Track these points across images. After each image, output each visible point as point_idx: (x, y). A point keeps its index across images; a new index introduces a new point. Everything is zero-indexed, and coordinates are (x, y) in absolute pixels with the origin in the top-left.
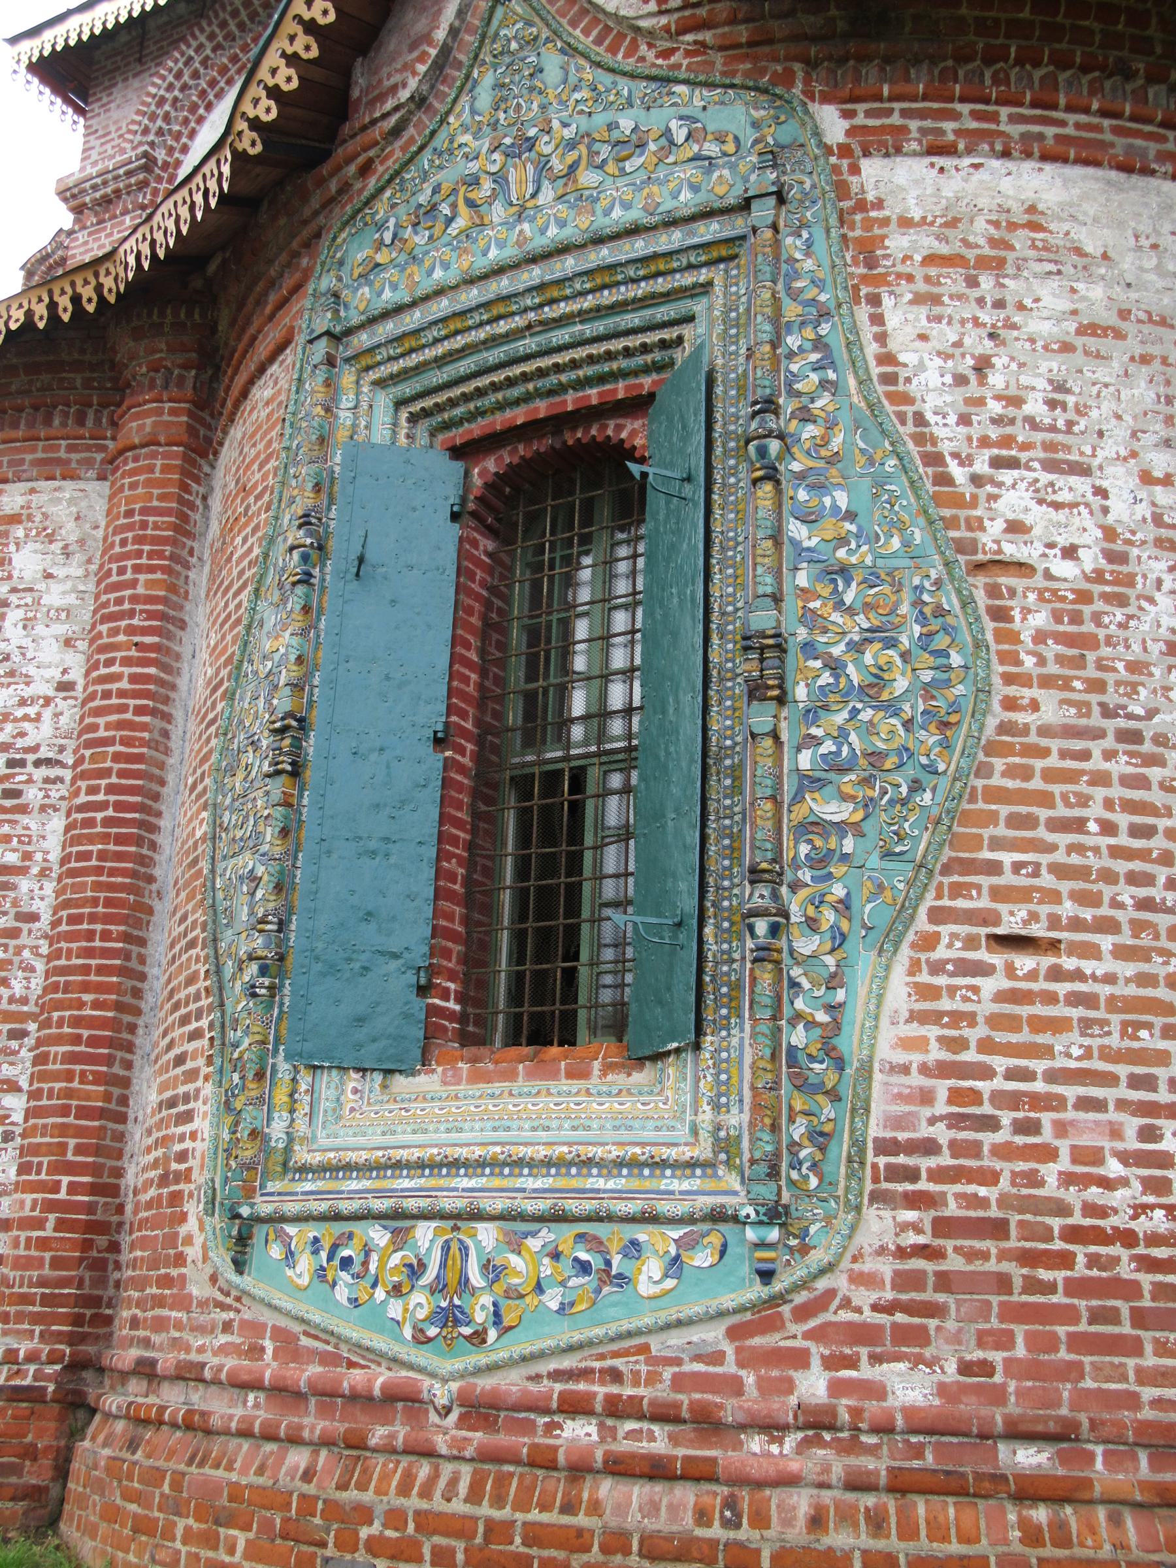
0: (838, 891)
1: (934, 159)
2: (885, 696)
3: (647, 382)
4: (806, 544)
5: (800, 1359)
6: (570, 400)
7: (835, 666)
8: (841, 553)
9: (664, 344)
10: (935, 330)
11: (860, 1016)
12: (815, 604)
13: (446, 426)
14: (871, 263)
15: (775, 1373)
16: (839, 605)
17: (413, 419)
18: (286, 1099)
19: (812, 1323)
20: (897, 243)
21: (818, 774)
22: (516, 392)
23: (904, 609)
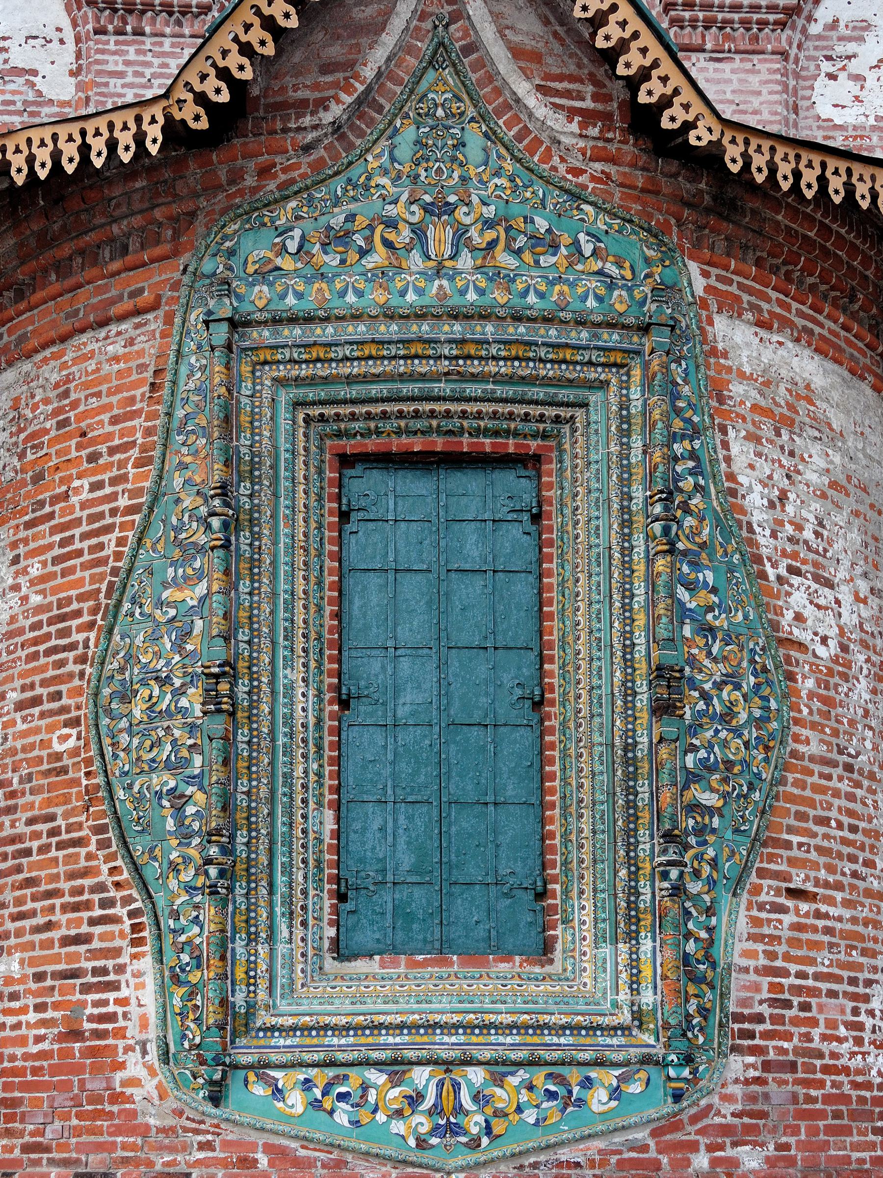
0: (711, 853)
1: (758, 330)
2: (734, 723)
3: (534, 444)
4: (688, 606)
5: (693, 1147)
6: (466, 443)
7: (706, 697)
8: (710, 616)
9: (557, 419)
10: (759, 462)
11: (723, 935)
12: (695, 651)
13: (339, 434)
14: (721, 400)
15: (679, 1156)
16: (709, 653)
17: (308, 420)
18: (243, 976)
19: (699, 1126)
20: (737, 389)
21: (697, 771)
22: (419, 424)
23: (745, 664)
